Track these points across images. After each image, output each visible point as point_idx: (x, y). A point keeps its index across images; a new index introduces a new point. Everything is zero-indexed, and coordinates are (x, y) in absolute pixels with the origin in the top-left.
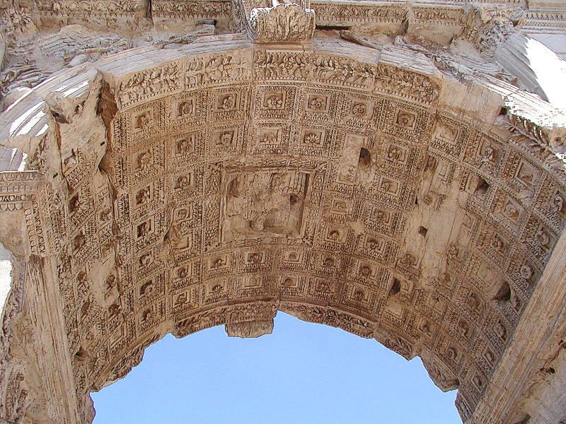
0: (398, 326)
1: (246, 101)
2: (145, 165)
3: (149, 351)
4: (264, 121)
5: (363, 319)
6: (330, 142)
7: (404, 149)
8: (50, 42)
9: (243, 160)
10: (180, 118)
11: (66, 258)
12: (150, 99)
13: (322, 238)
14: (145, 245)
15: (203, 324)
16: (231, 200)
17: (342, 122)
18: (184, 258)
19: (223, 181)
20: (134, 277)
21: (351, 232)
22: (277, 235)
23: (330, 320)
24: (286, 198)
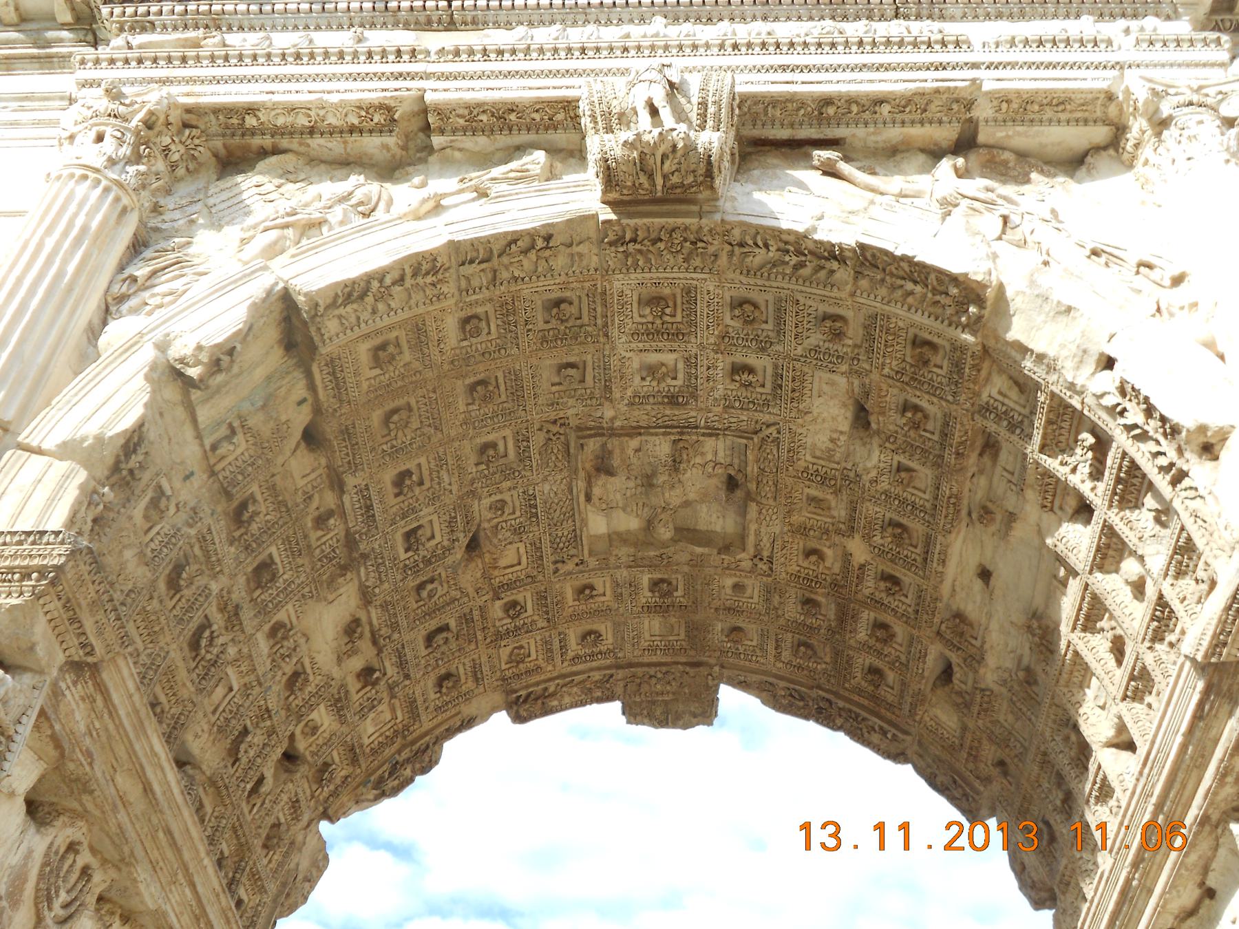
0: (952, 749)
1: (599, 309)
2: (400, 434)
3: (453, 749)
4: (641, 345)
5: (885, 726)
6: (780, 387)
7: (932, 409)
8: (231, 194)
9: (609, 413)
10: (465, 343)
11: (230, 608)
12: (387, 321)
13: (791, 563)
14: (421, 565)
15: (567, 700)
16: (600, 483)
17: (799, 351)
18: (510, 586)
19: (572, 451)
20: (403, 623)
21: (847, 557)
22: (699, 550)
23: (825, 715)
24: (714, 481)
